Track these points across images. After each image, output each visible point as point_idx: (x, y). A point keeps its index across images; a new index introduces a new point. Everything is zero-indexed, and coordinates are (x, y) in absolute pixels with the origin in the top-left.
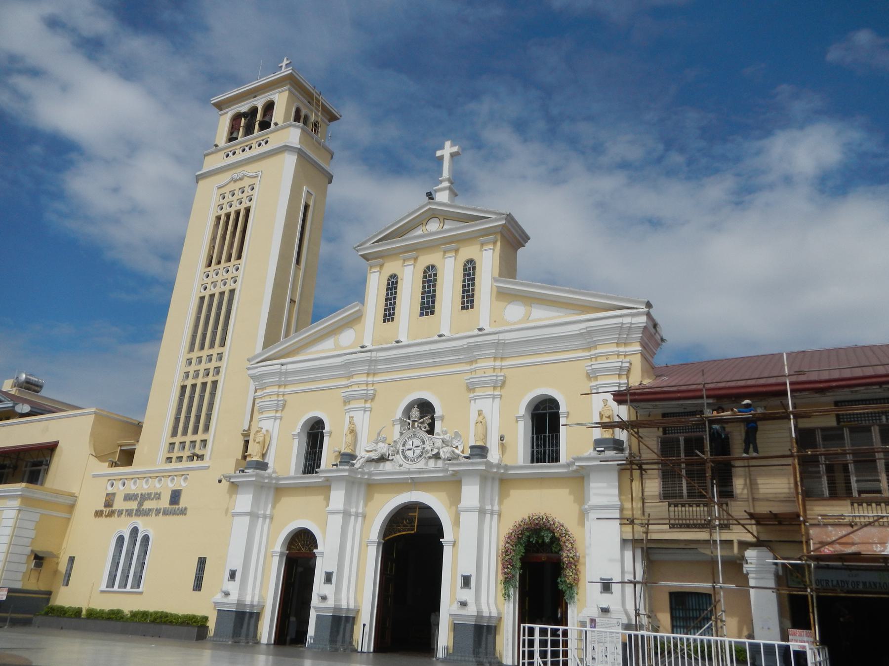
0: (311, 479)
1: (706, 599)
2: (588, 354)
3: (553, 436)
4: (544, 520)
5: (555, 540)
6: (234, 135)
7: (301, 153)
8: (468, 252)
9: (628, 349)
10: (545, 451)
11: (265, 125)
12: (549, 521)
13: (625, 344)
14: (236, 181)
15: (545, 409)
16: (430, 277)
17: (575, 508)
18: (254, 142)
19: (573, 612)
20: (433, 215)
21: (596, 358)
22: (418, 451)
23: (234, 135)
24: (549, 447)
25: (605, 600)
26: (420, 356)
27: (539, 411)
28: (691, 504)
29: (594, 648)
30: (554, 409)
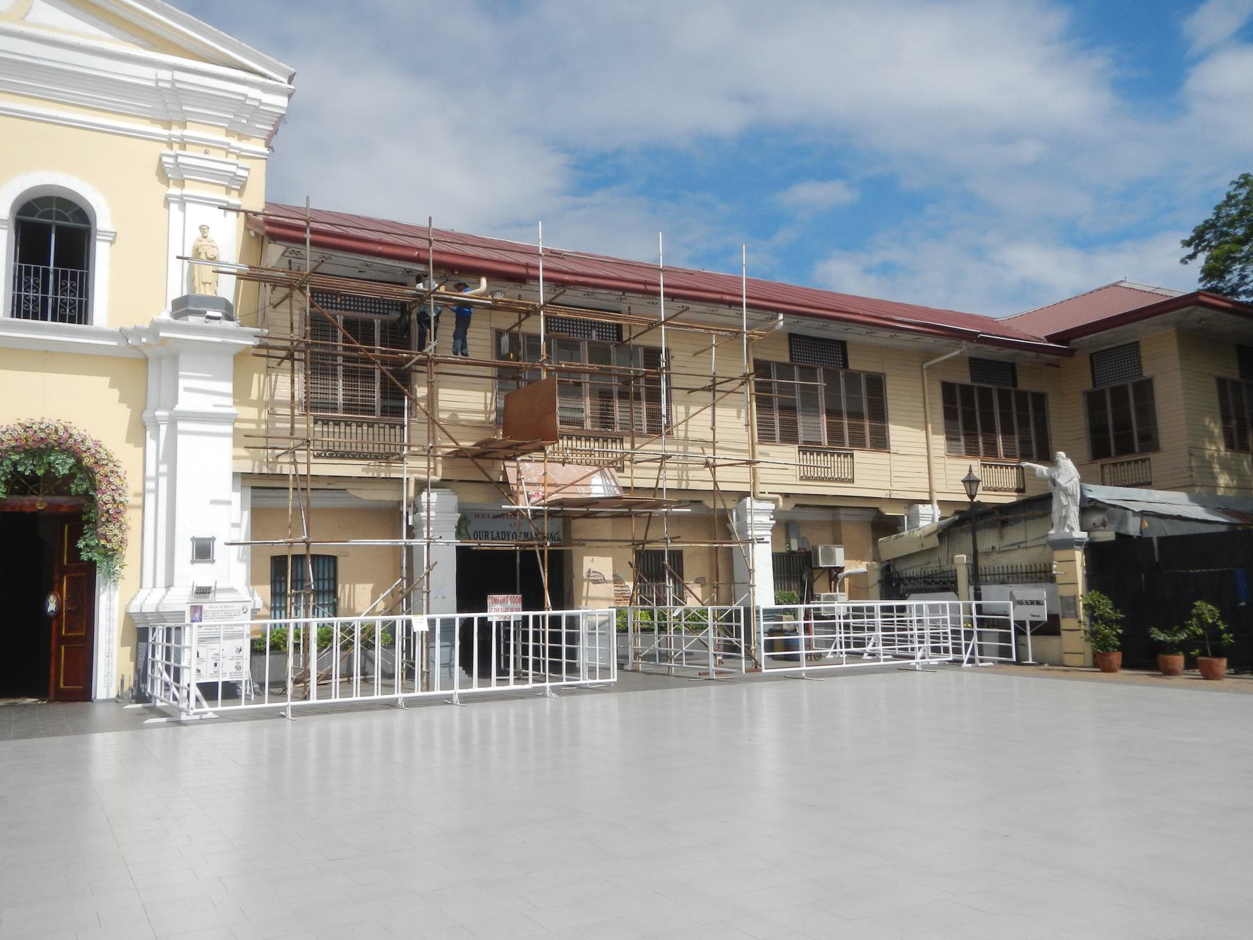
1: (324, 562)
2: (158, 130)
3: (64, 274)
4: (61, 433)
5: (89, 473)
9: (245, 145)
10: (45, 300)
12: (71, 436)
13: (241, 137)
15: (47, 215)
17: (123, 414)
19: (110, 598)
21: (183, 146)
24: (56, 292)
25: (203, 574)
27: (33, 216)
28: (350, 423)
29: (198, 654)
30: (66, 219)
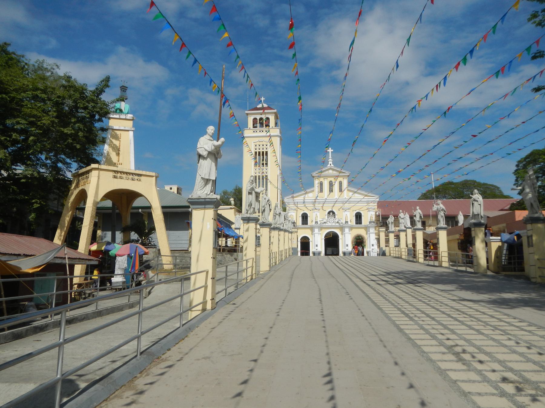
0: (305, 226)
6: (255, 125)
7: (280, 137)
8: (340, 179)
11: (268, 125)
13: (375, 203)
14: (260, 142)
16: (331, 185)
17: (365, 232)
18: (264, 130)
20: (331, 169)
22: (333, 221)
23: (255, 125)
25: (373, 248)
26: (331, 202)
